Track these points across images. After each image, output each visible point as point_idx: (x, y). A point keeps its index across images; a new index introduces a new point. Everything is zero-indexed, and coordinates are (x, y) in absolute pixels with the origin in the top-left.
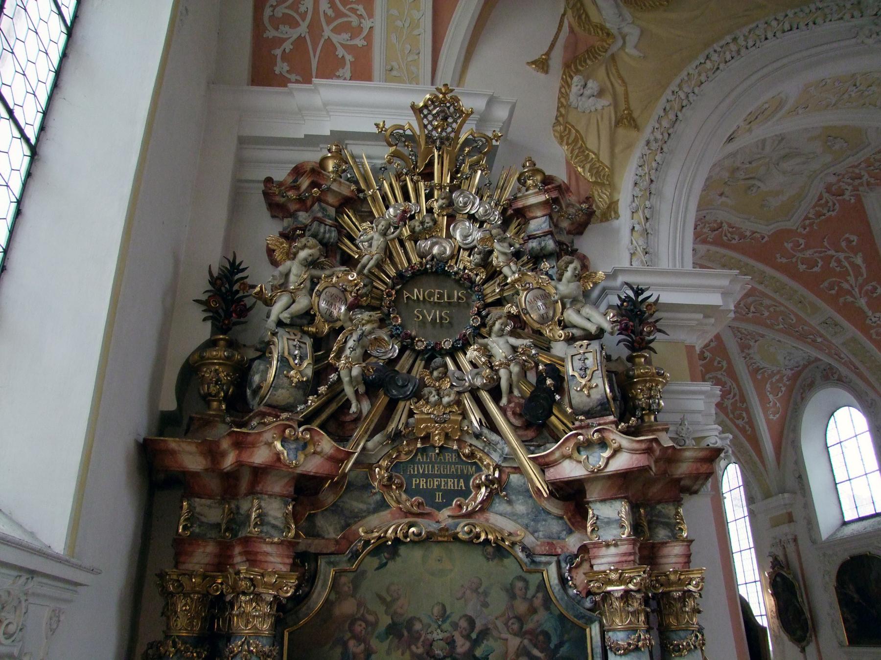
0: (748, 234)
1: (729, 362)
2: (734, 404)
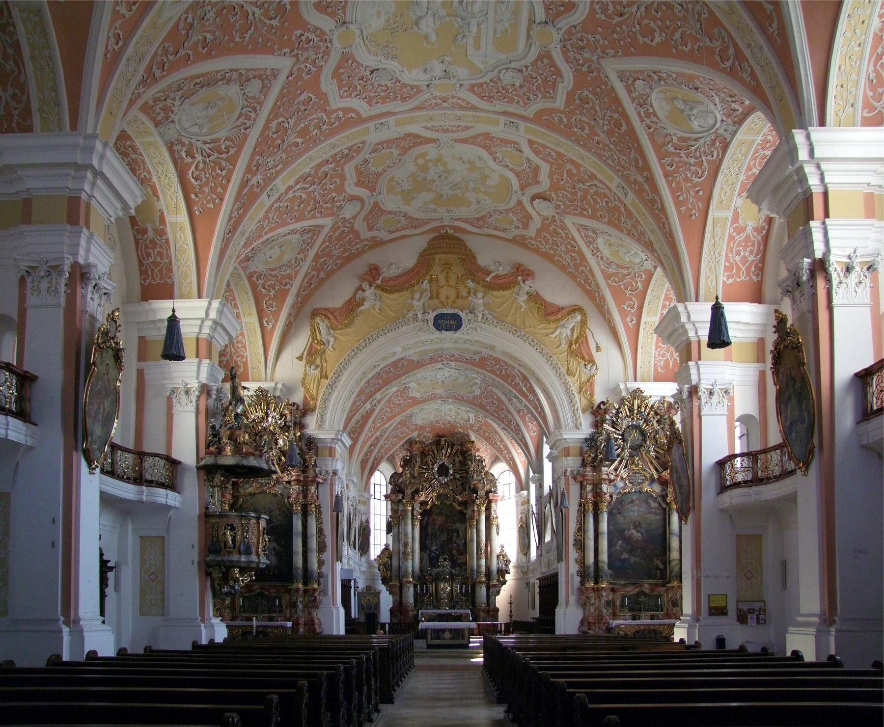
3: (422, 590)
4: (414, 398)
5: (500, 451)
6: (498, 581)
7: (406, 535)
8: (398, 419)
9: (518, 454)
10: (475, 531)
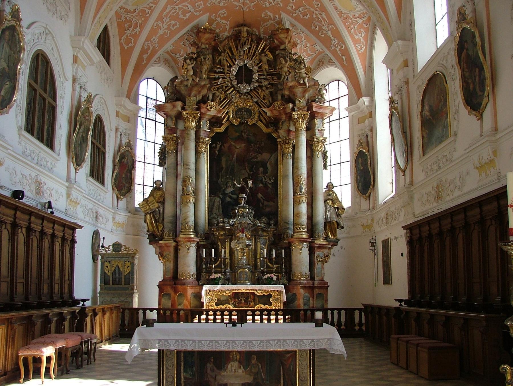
3: (209, 254)
5: (326, 41)
6: (326, 238)
7: (186, 165)
9: (356, 42)
10: (290, 162)
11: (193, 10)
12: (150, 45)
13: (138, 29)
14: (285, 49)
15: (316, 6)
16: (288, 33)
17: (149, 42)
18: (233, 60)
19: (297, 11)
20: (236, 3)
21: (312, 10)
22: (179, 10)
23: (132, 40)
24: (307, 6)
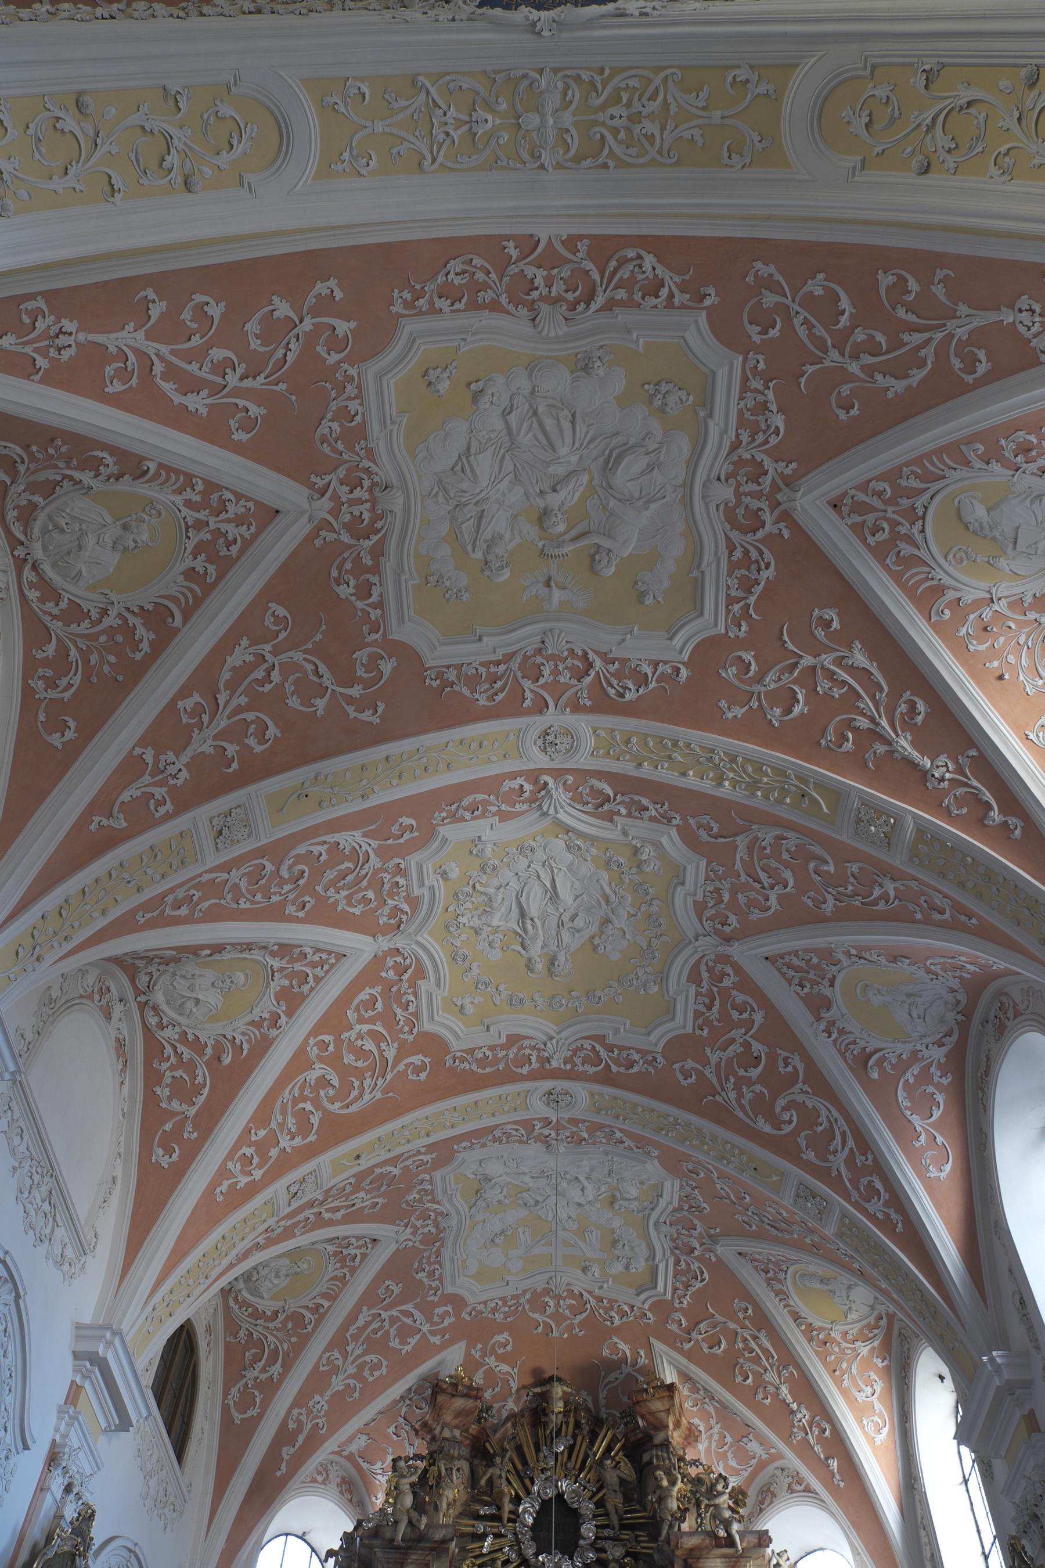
0: (647, 669)
1: (806, 1057)
2: (850, 1161)
4: (432, 1045)
8: (370, 1147)
9: (861, 1411)
11: (425, 1328)
12: (303, 1418)
13: (276, 1369)
14: (666, 1445)
15: (741, 1315)
16: (672, 1397)
17: (303, 1411)
18: (527, 1482)
19: (694, 1334)
20: (536, 1316)
21: (732, 1326)
22: (391, 1326)
23: (258, 1400)
24: (718, 1317)
